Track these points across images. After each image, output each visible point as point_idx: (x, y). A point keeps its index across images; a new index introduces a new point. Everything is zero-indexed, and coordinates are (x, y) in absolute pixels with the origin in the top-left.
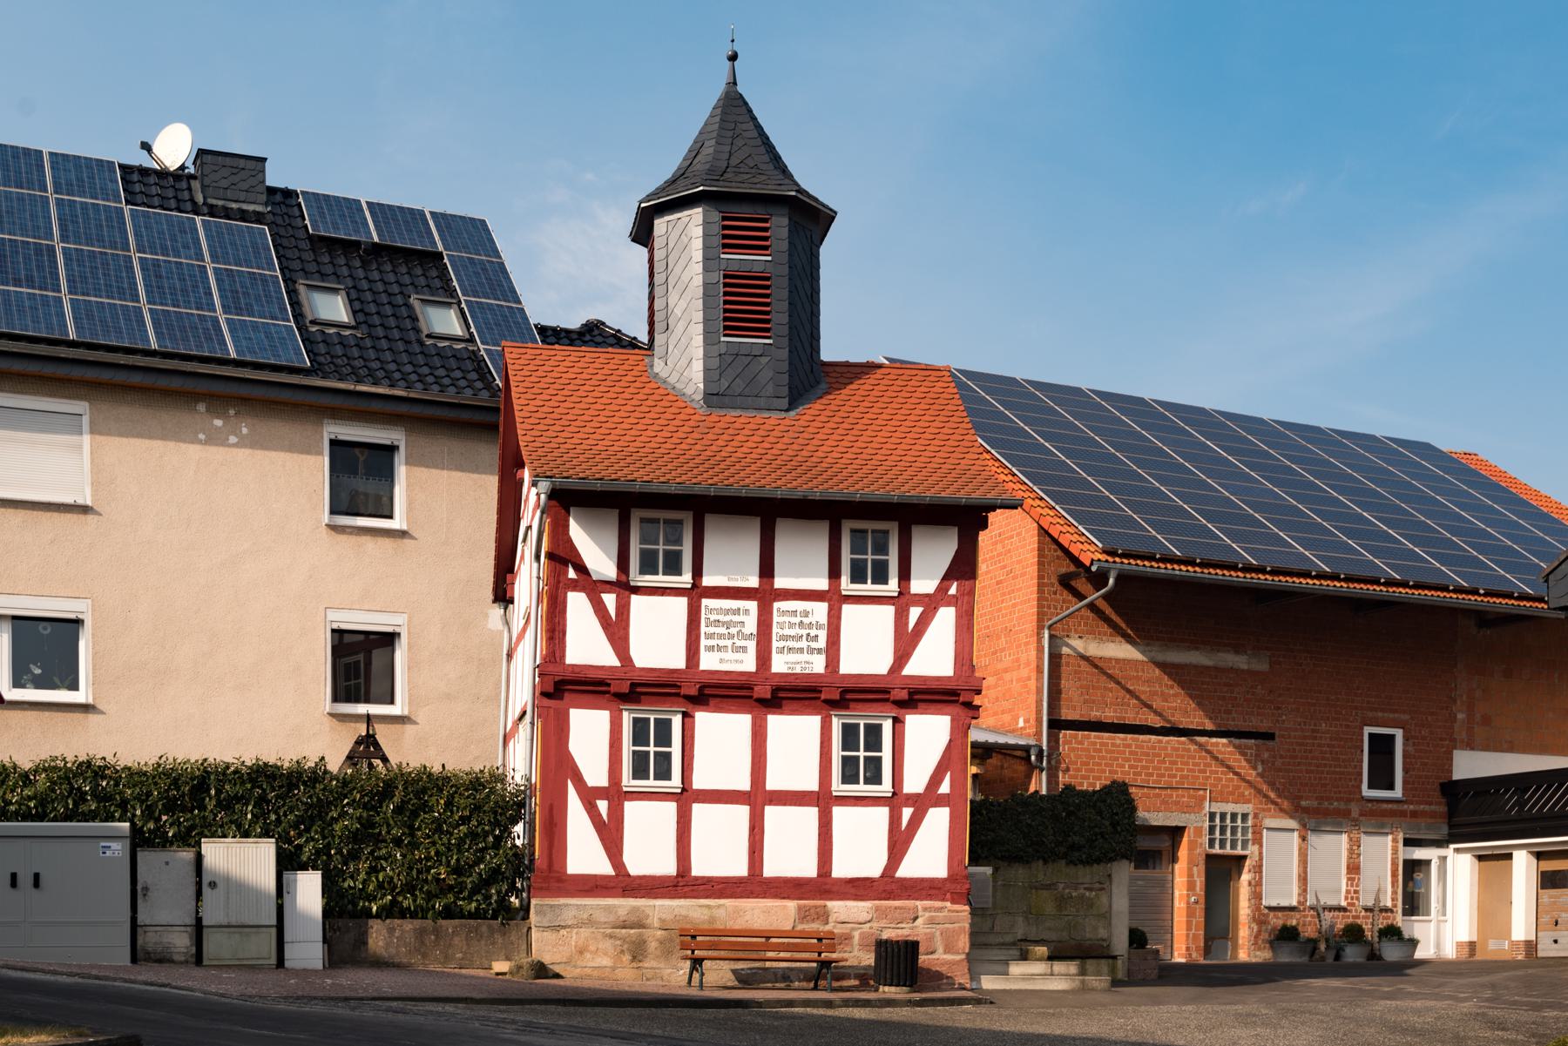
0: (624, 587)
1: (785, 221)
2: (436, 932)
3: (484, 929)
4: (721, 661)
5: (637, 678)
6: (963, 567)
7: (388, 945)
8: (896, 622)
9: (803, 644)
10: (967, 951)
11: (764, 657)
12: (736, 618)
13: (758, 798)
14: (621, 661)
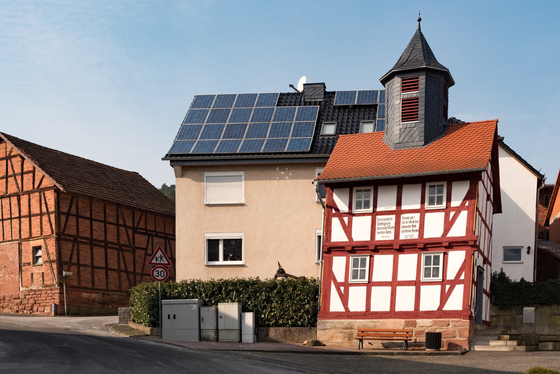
0: (351, 214)
1: (424, 77)
2: (290, 331)
3: (304, 330)
4: (382, 237)
5: (354, 245)
6: (472, 195)
7: (275, 336)
8: (445, 218)
9: (411, 229)
10: (468, 336)
11: (397, 235)
12: (388, 222)
13: (394, 284)
14: (349, 240)
